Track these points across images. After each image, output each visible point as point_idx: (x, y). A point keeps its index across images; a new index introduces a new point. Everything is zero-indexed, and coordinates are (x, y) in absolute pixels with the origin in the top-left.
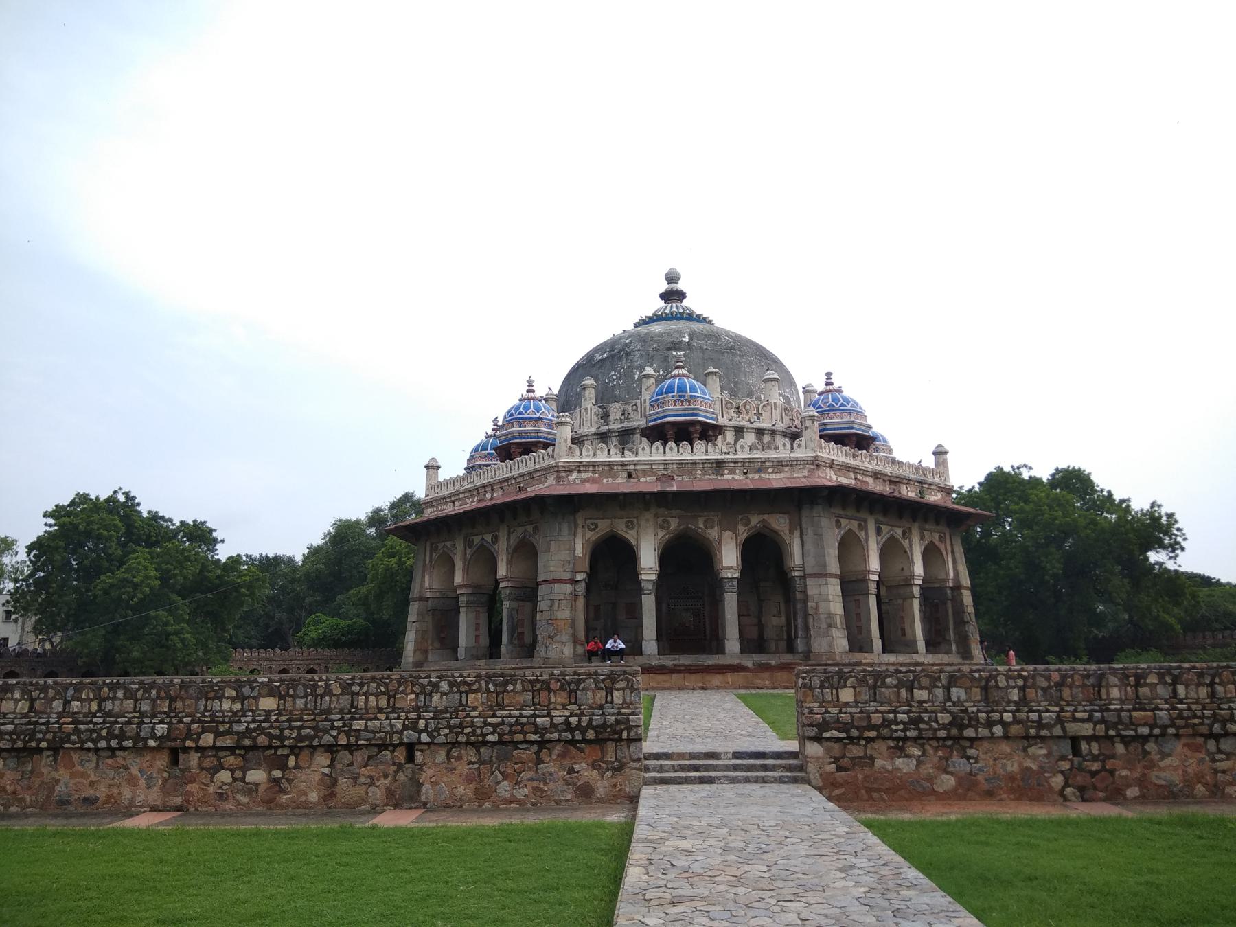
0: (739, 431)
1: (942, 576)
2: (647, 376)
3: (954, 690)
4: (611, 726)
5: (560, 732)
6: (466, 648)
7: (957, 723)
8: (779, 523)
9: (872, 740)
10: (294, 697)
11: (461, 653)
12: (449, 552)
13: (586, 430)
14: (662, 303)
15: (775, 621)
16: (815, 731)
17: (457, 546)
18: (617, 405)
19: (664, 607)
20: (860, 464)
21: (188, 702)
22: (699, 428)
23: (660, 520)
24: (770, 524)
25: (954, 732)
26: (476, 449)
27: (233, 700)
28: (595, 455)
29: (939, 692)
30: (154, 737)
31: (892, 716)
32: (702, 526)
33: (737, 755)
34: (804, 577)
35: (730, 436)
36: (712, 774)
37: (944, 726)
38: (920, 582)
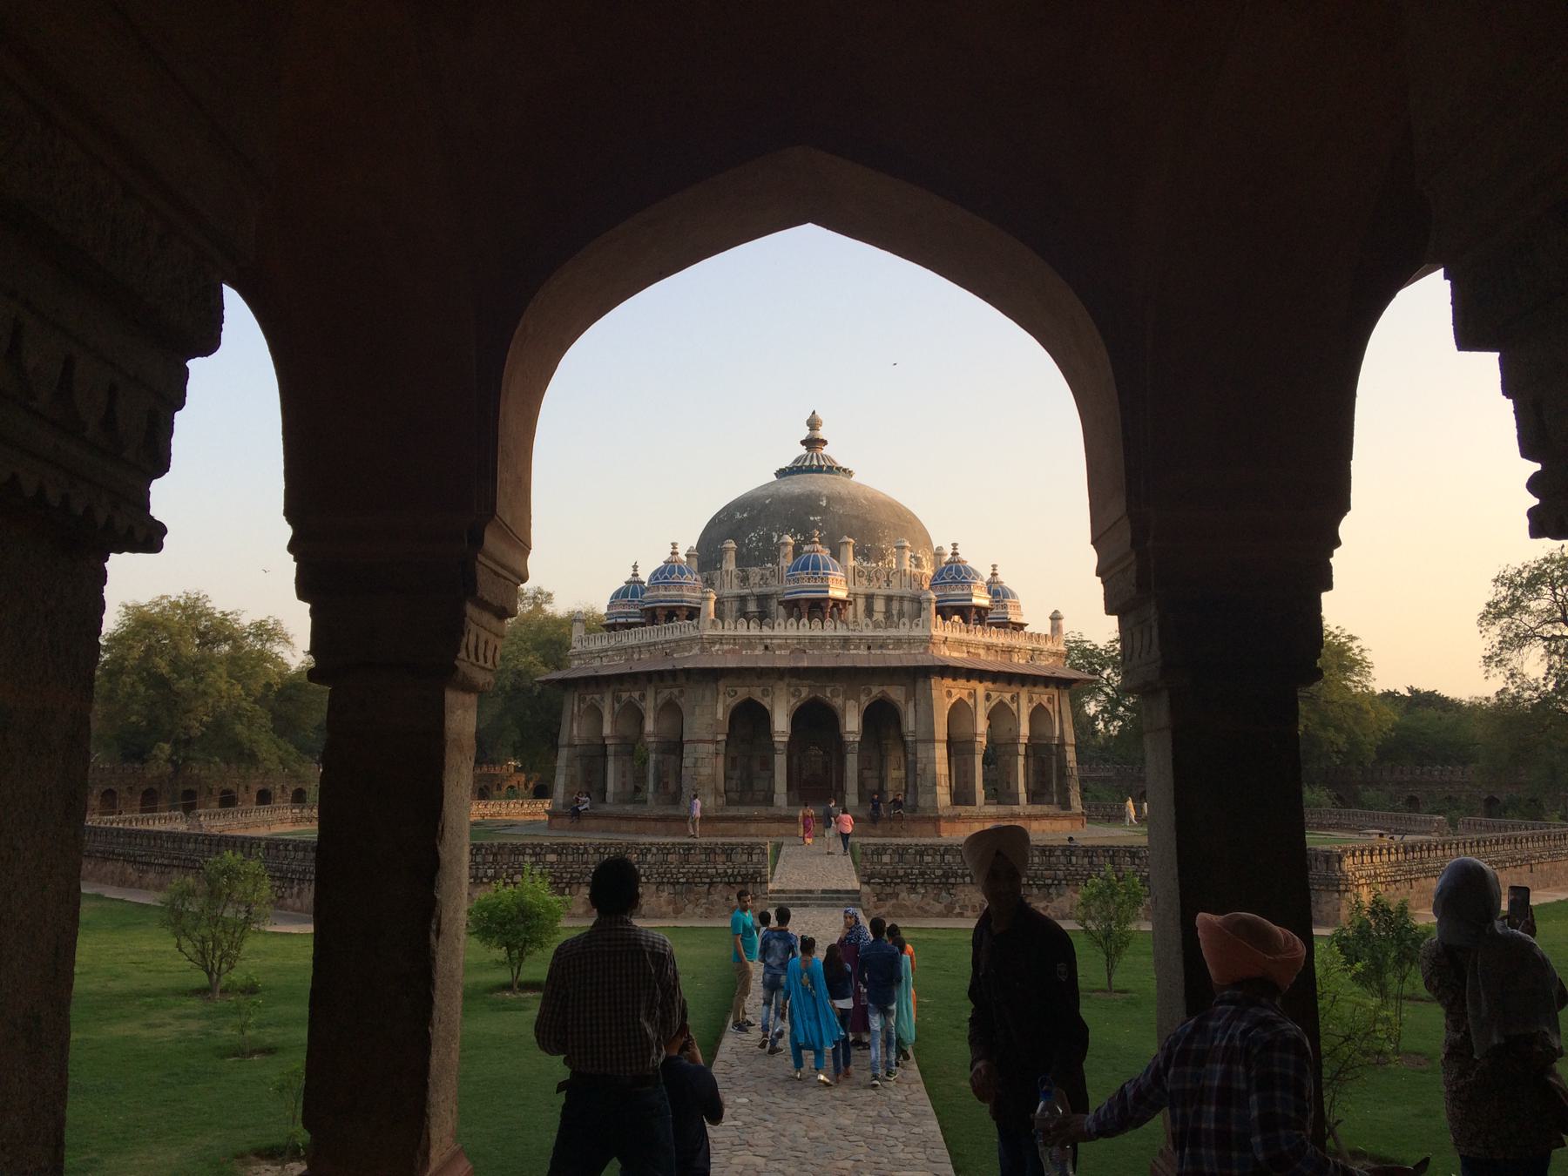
0: (870, 598)
1: (1048, 734)
2: (786, 544)
3: (946, 857)
4: (752, 875)
5: (721, 878)
6: (614, 793)
7: (946, 875)
8: (896, 694)
9: (898, 884)
10: (567, 854)
11: (609, 797)
12: (597, 704)
13: (727, 591)
14: (803, 450)
15: (895, 774)
16: (867, 879)
17: (606, 701)
18: (756, 569)
19: (795, 760)
20: (973, 638)
21: (504, 856)
22: (831, 604)
23: (792, 689)
24: (888, 694)
25: (944, 880)
26: (617, 595)
27: (531, 855)
28: (736, 628)
29: (938, 858)
30: (486, 876)
31: (910, 871)
32: (829, 695)
33: (824, 891)
34: (916, 741)
35: (861, 603)
36: (808, 902)
37: (937, 877)
38: (1026, 741)
